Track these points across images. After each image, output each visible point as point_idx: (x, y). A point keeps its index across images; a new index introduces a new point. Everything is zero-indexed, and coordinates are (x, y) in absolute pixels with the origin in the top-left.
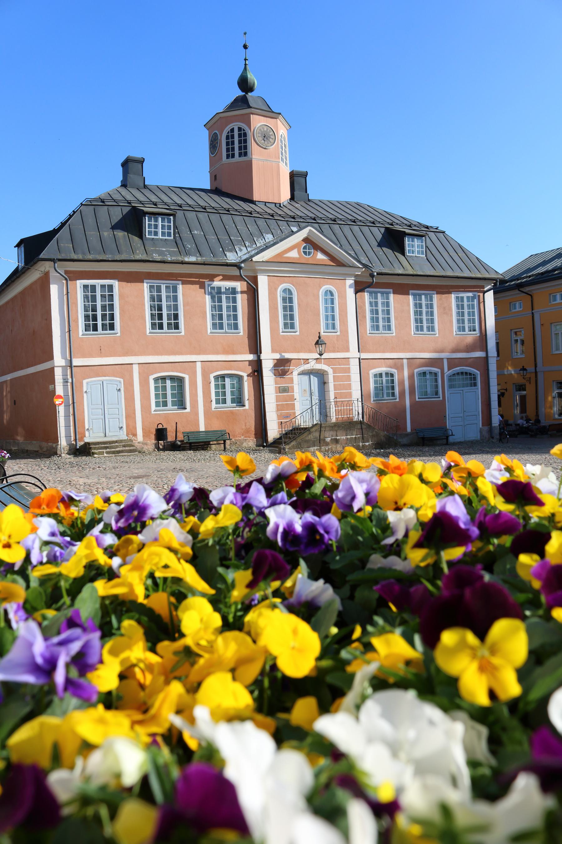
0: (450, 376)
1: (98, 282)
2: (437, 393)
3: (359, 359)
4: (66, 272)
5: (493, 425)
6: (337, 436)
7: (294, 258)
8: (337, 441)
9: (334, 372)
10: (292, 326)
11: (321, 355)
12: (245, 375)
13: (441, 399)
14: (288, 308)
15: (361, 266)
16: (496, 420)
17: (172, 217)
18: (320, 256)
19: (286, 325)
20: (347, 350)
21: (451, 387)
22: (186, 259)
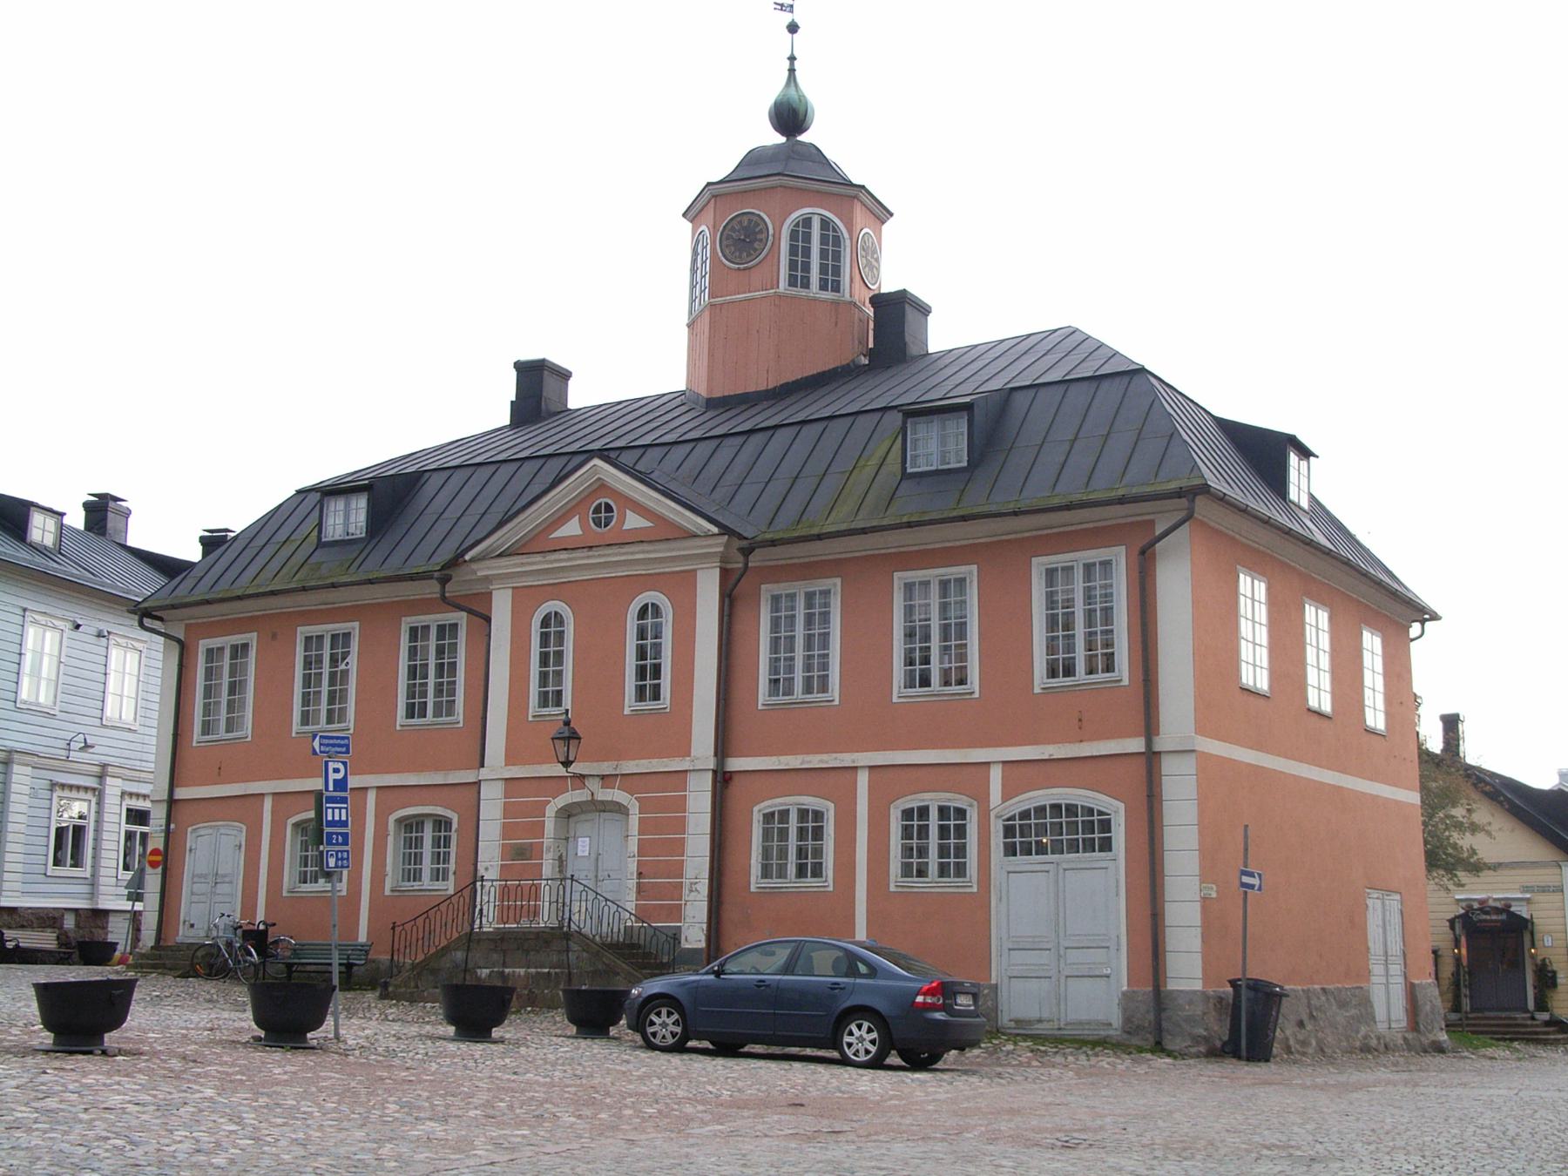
0: (1012, 818)
3: (715, 772)
5: (1172, 986)
6: (504, 965)
15: (715, 530)
21: (1010, 850)
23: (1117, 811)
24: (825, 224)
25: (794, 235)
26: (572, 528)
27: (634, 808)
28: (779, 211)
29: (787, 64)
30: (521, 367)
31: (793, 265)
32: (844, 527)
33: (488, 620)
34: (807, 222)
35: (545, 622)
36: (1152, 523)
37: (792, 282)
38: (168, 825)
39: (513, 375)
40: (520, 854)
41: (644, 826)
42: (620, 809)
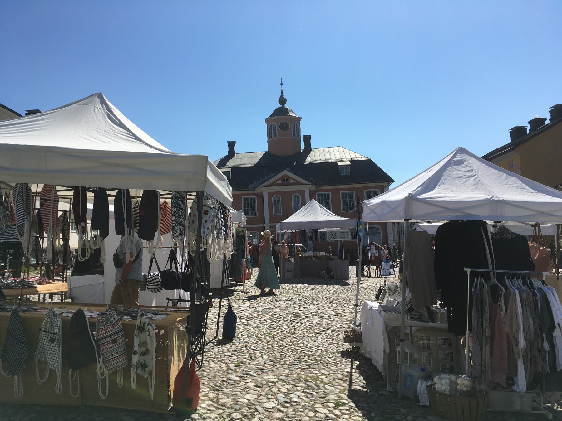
33: (263, 198)
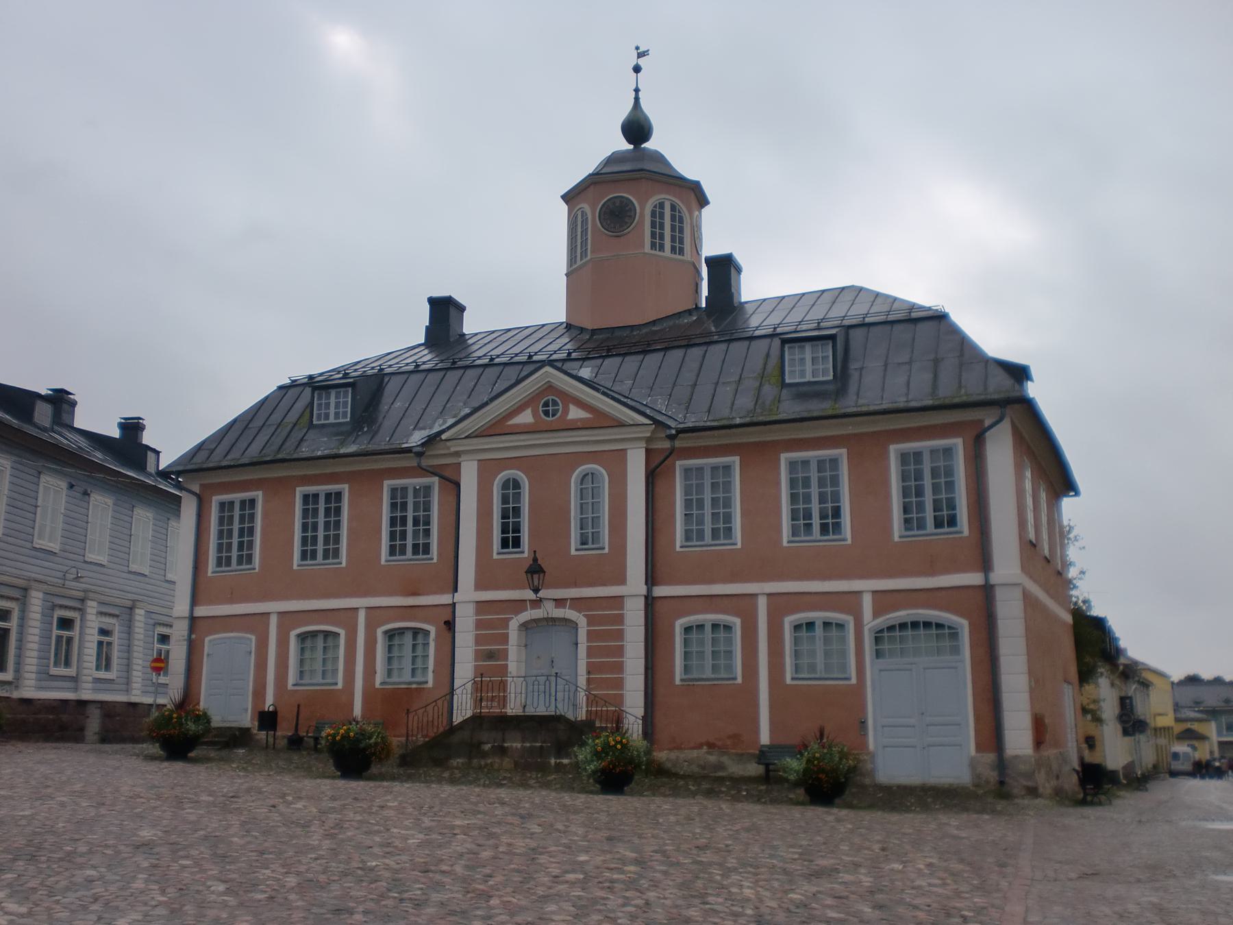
0: (882, 631)
1: (237, 496)
2: (844, 667)
3: (646, 597)
4: (202, 486)
7: (525, 425)
8: (502, 751)
9: (591, 621)
10: (517, 543)
11: (536, 591)
12: (432, 629)
13: (854, 681)
14: (510, 514)
16: (1018, 738)
17: (350, 390)
18: (575, 413)
19: (505, 543)
20: (621, 580)
21: (878, 654)
22: (342, 451)
23: (963, 624)
24: (673, 208)
25: (653, 214)
26: (526, 417)
27: (582, 621)
28: (633, 198)
29: (634, 93)
30: (433, 302)
31: (653, 235)
32: (747, 420)
33: (458, 485)
34: (662, 205)
35: (505, 485)
36: (981, 422)
37: (653, 246)
38: (190, 636)
39: (427, 307)
40: (491, 656)
41: (591, 635)
42: (571, 625)
